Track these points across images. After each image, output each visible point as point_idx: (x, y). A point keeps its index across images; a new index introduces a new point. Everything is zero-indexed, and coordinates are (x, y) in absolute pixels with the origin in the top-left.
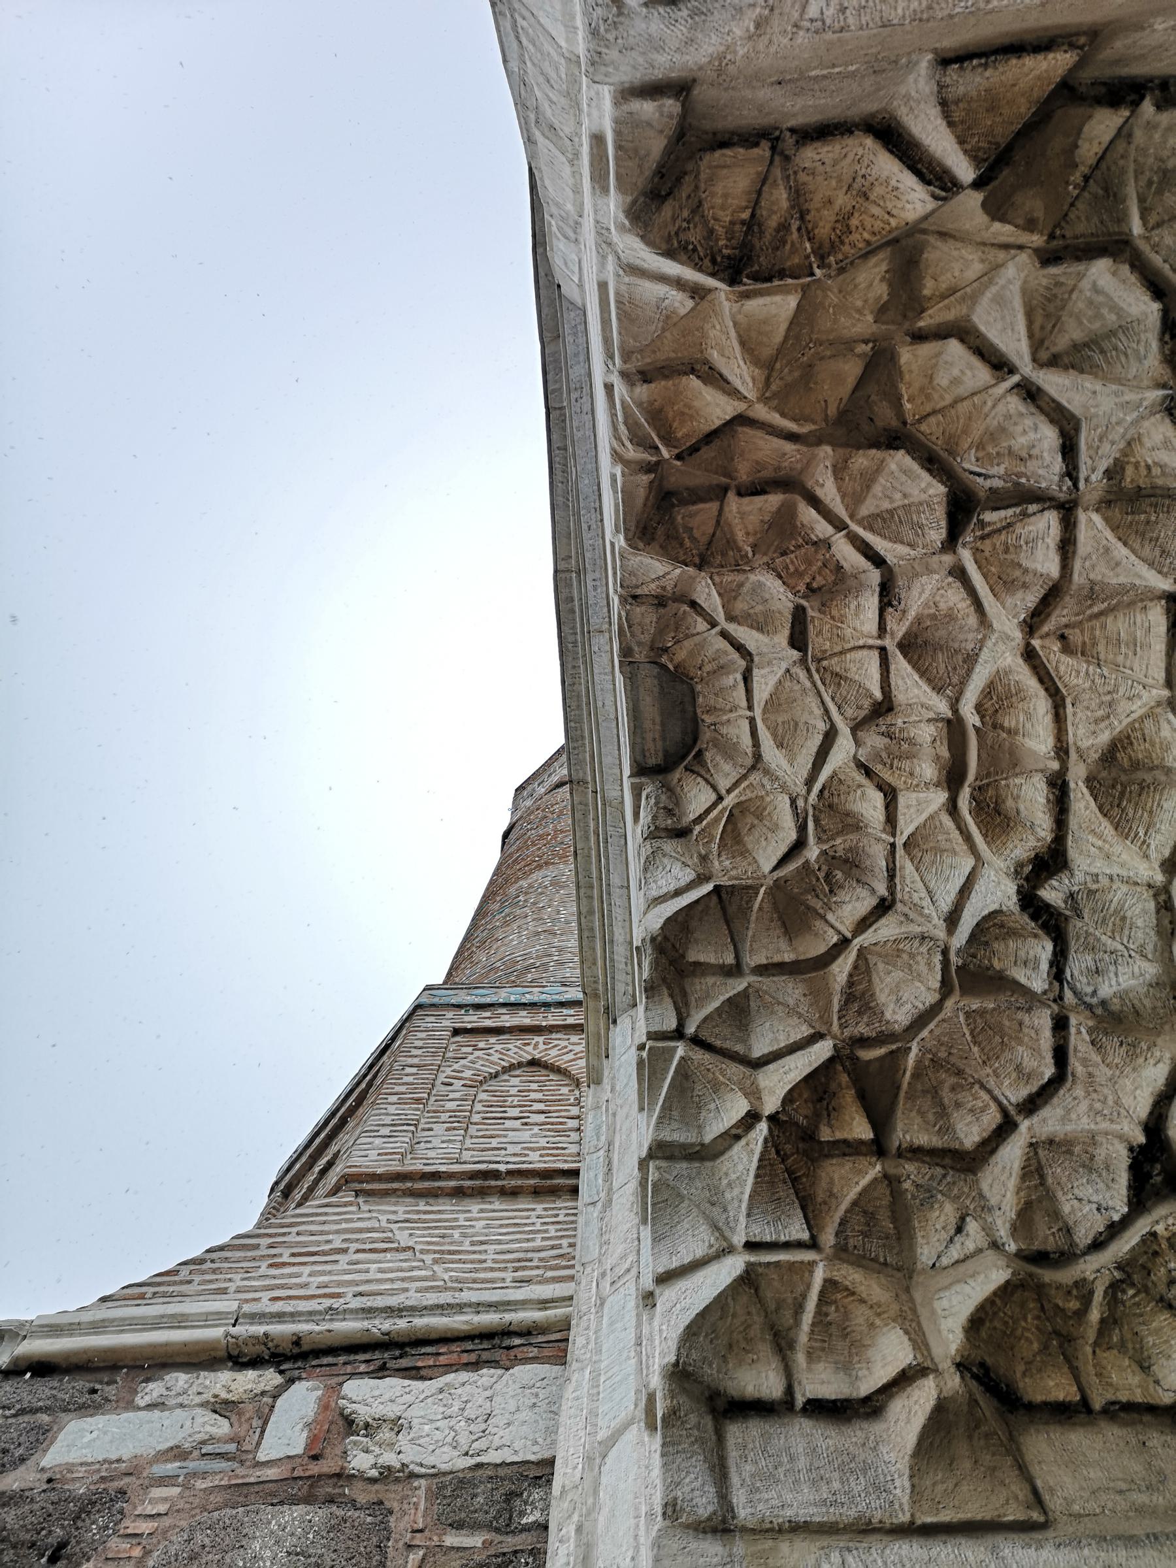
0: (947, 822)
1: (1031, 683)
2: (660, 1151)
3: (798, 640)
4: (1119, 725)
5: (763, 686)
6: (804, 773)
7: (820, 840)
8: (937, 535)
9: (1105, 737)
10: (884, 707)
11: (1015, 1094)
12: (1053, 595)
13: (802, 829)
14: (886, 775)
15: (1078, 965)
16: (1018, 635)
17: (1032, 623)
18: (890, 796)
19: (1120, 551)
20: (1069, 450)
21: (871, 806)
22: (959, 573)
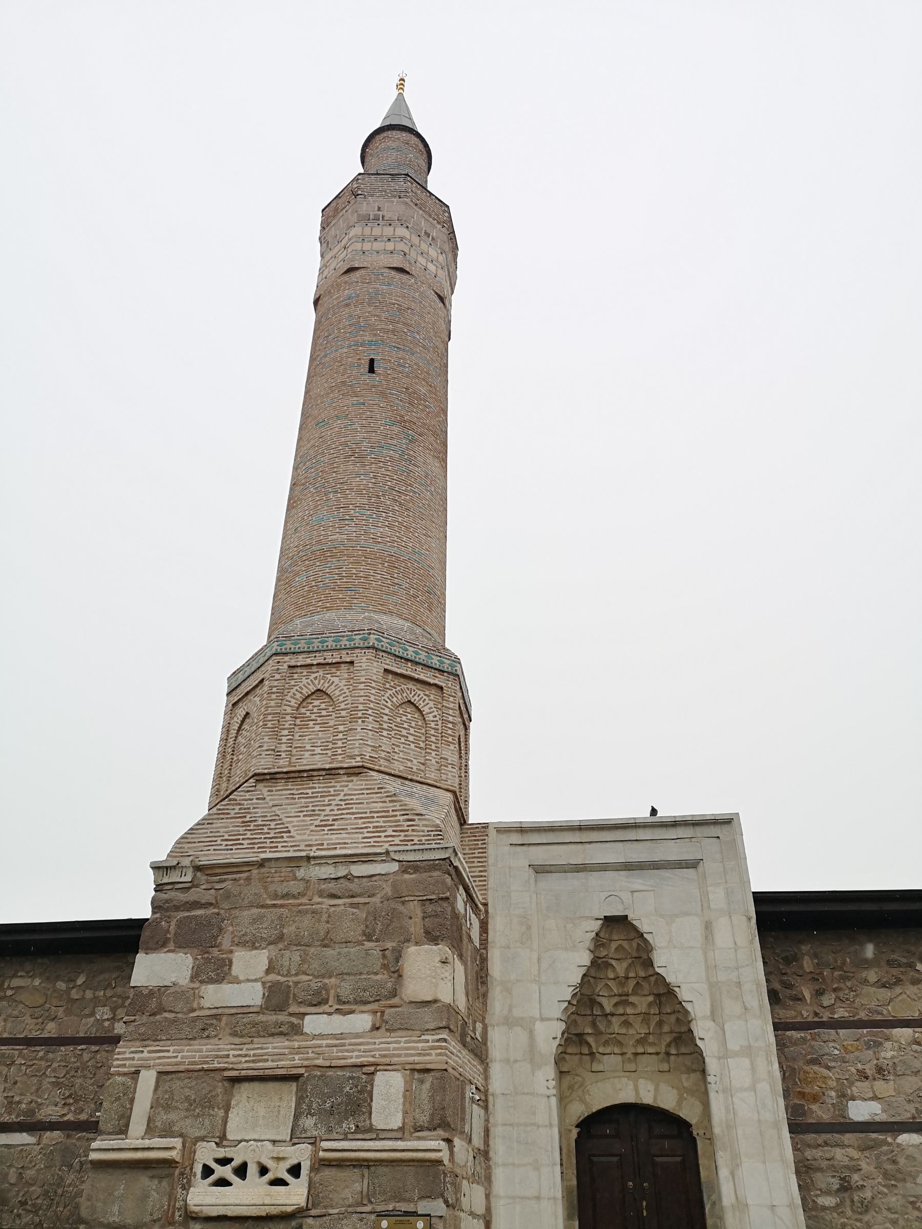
0: (613, 994)
1: (637, 1013)
2: (569, 1002)
3: (635, 958)
4: (633, 1024)
5: (625, 944)
6: (612, 957)
7: (602, 962)
8: (655, 992)
9: (631, 1022)
10: (627, 978)
11: (579, 1013)
12: (649, 1014)
13: (603, 958)
14: (617, 980)
15: (599, 1018)
16: (643, 1011)
17: (645, 1013)
18: (614, 979)
19: (654, 1023)
20: (667, 1014)
21: (611, 975)
22: (650, 994)
